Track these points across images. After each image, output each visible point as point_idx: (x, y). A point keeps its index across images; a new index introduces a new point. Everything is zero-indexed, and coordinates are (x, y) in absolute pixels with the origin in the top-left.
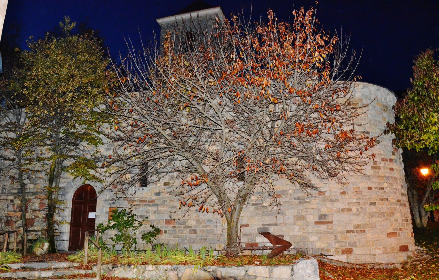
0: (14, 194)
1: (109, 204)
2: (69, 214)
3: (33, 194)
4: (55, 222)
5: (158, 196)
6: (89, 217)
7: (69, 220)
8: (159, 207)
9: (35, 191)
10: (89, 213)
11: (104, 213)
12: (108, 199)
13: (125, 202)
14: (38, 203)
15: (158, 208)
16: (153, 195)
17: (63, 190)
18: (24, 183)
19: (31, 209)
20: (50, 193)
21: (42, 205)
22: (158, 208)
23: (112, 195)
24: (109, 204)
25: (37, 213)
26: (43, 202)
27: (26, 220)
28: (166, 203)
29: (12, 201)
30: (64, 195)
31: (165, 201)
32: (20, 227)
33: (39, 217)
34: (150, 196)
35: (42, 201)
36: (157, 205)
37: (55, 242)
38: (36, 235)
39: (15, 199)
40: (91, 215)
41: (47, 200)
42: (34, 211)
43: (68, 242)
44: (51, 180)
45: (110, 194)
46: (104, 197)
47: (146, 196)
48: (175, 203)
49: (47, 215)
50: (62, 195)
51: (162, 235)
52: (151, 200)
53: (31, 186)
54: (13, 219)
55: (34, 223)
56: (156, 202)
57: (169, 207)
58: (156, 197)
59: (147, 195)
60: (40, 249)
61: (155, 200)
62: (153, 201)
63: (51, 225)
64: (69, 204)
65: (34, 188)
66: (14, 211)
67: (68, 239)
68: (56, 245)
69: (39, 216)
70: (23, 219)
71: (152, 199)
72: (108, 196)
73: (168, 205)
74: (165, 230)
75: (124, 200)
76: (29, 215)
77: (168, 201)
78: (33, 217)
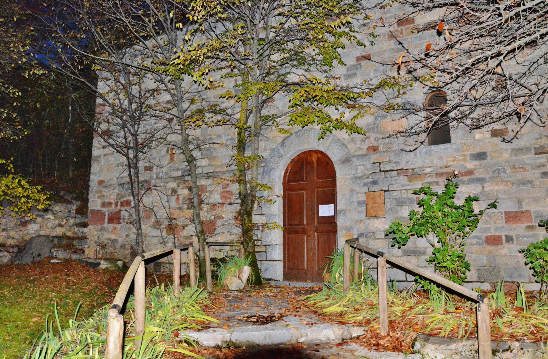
0: (175, 178)
1: (365, 185)
2: (279, 210)
3: (209, 176)
4: (254, 225)
5: (480, 160)
6: (321, 214)
7: (279, 220)
8: (486, 185)
9: (212, 170)
10: (320, 206)
11: (356, 205)
12: (360, 175)
13: (401, 178)
14: (219, 192)
15: (483, 187)
16: (468, 158)
17: (263, 165)
18: (192, 156)
19: (208, 204)
20: (241, 171)
21: (226, 194)
22: (483, 187)
23: (369, 166)
24: (365, 185)
25: (219, 211)
26: (227, 189)
27: (201, 223)
28: (502, 175)
29: (174, 191)
30: (267, 172)
31: (499, 170)
32: (192, 236)
33: (223, 218)
34: (462, 163)
35: (225, 188)
36: (481, 180)
37: (259, 263)
38: (220, 251)
39: (179, 186)
40: (325, 210)
41: (237, 184)
42: (213, 206)
43: (281, 264)
44: (241, 146)
45: (364, 166)
46: (353, 172)
47: (449, 164)
48: (526, 173)
49: (239, 213)
50: (262, 174)
51: (499, 247)
52: (464, 170)
53: (204, 162)
54: (178, 223)
55: (215, 229)
56: (477, 175)
57: (513, 184)
58: (477, 163)
59: (454, 161)
60: (235, 279)
61: (475, 169)
62: (470, 172)
63: (249, 231)
64: (279, 190)
65: (209, 165)
66: (180, 209)
67: (282, 258)
68: (260, 270)
69: (223, 216)
70: (196, 222)
71: (466, 167)
72: (360, 168)
73: (510, 179)
74: (506, 236)
75: (398, 174)
76: (205, 215)
77: (509, 171)
78: (213, 217)
